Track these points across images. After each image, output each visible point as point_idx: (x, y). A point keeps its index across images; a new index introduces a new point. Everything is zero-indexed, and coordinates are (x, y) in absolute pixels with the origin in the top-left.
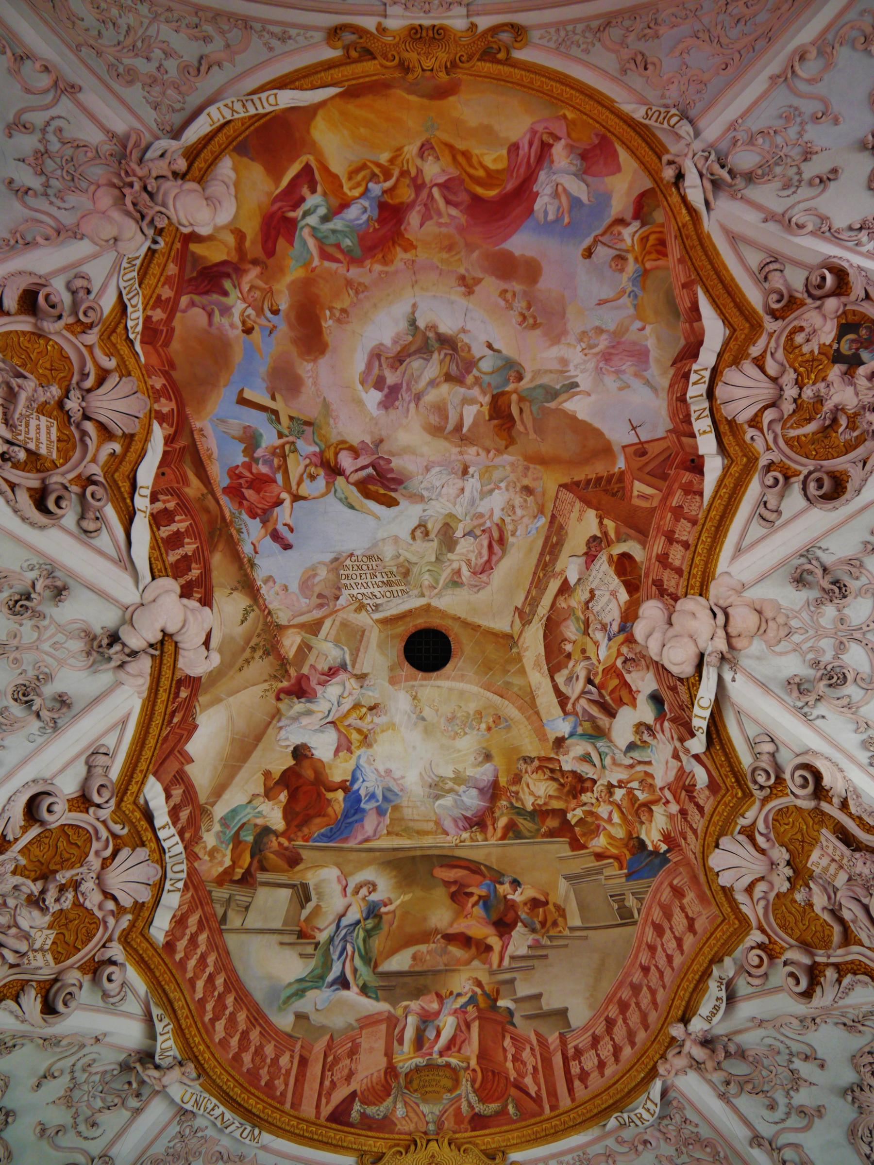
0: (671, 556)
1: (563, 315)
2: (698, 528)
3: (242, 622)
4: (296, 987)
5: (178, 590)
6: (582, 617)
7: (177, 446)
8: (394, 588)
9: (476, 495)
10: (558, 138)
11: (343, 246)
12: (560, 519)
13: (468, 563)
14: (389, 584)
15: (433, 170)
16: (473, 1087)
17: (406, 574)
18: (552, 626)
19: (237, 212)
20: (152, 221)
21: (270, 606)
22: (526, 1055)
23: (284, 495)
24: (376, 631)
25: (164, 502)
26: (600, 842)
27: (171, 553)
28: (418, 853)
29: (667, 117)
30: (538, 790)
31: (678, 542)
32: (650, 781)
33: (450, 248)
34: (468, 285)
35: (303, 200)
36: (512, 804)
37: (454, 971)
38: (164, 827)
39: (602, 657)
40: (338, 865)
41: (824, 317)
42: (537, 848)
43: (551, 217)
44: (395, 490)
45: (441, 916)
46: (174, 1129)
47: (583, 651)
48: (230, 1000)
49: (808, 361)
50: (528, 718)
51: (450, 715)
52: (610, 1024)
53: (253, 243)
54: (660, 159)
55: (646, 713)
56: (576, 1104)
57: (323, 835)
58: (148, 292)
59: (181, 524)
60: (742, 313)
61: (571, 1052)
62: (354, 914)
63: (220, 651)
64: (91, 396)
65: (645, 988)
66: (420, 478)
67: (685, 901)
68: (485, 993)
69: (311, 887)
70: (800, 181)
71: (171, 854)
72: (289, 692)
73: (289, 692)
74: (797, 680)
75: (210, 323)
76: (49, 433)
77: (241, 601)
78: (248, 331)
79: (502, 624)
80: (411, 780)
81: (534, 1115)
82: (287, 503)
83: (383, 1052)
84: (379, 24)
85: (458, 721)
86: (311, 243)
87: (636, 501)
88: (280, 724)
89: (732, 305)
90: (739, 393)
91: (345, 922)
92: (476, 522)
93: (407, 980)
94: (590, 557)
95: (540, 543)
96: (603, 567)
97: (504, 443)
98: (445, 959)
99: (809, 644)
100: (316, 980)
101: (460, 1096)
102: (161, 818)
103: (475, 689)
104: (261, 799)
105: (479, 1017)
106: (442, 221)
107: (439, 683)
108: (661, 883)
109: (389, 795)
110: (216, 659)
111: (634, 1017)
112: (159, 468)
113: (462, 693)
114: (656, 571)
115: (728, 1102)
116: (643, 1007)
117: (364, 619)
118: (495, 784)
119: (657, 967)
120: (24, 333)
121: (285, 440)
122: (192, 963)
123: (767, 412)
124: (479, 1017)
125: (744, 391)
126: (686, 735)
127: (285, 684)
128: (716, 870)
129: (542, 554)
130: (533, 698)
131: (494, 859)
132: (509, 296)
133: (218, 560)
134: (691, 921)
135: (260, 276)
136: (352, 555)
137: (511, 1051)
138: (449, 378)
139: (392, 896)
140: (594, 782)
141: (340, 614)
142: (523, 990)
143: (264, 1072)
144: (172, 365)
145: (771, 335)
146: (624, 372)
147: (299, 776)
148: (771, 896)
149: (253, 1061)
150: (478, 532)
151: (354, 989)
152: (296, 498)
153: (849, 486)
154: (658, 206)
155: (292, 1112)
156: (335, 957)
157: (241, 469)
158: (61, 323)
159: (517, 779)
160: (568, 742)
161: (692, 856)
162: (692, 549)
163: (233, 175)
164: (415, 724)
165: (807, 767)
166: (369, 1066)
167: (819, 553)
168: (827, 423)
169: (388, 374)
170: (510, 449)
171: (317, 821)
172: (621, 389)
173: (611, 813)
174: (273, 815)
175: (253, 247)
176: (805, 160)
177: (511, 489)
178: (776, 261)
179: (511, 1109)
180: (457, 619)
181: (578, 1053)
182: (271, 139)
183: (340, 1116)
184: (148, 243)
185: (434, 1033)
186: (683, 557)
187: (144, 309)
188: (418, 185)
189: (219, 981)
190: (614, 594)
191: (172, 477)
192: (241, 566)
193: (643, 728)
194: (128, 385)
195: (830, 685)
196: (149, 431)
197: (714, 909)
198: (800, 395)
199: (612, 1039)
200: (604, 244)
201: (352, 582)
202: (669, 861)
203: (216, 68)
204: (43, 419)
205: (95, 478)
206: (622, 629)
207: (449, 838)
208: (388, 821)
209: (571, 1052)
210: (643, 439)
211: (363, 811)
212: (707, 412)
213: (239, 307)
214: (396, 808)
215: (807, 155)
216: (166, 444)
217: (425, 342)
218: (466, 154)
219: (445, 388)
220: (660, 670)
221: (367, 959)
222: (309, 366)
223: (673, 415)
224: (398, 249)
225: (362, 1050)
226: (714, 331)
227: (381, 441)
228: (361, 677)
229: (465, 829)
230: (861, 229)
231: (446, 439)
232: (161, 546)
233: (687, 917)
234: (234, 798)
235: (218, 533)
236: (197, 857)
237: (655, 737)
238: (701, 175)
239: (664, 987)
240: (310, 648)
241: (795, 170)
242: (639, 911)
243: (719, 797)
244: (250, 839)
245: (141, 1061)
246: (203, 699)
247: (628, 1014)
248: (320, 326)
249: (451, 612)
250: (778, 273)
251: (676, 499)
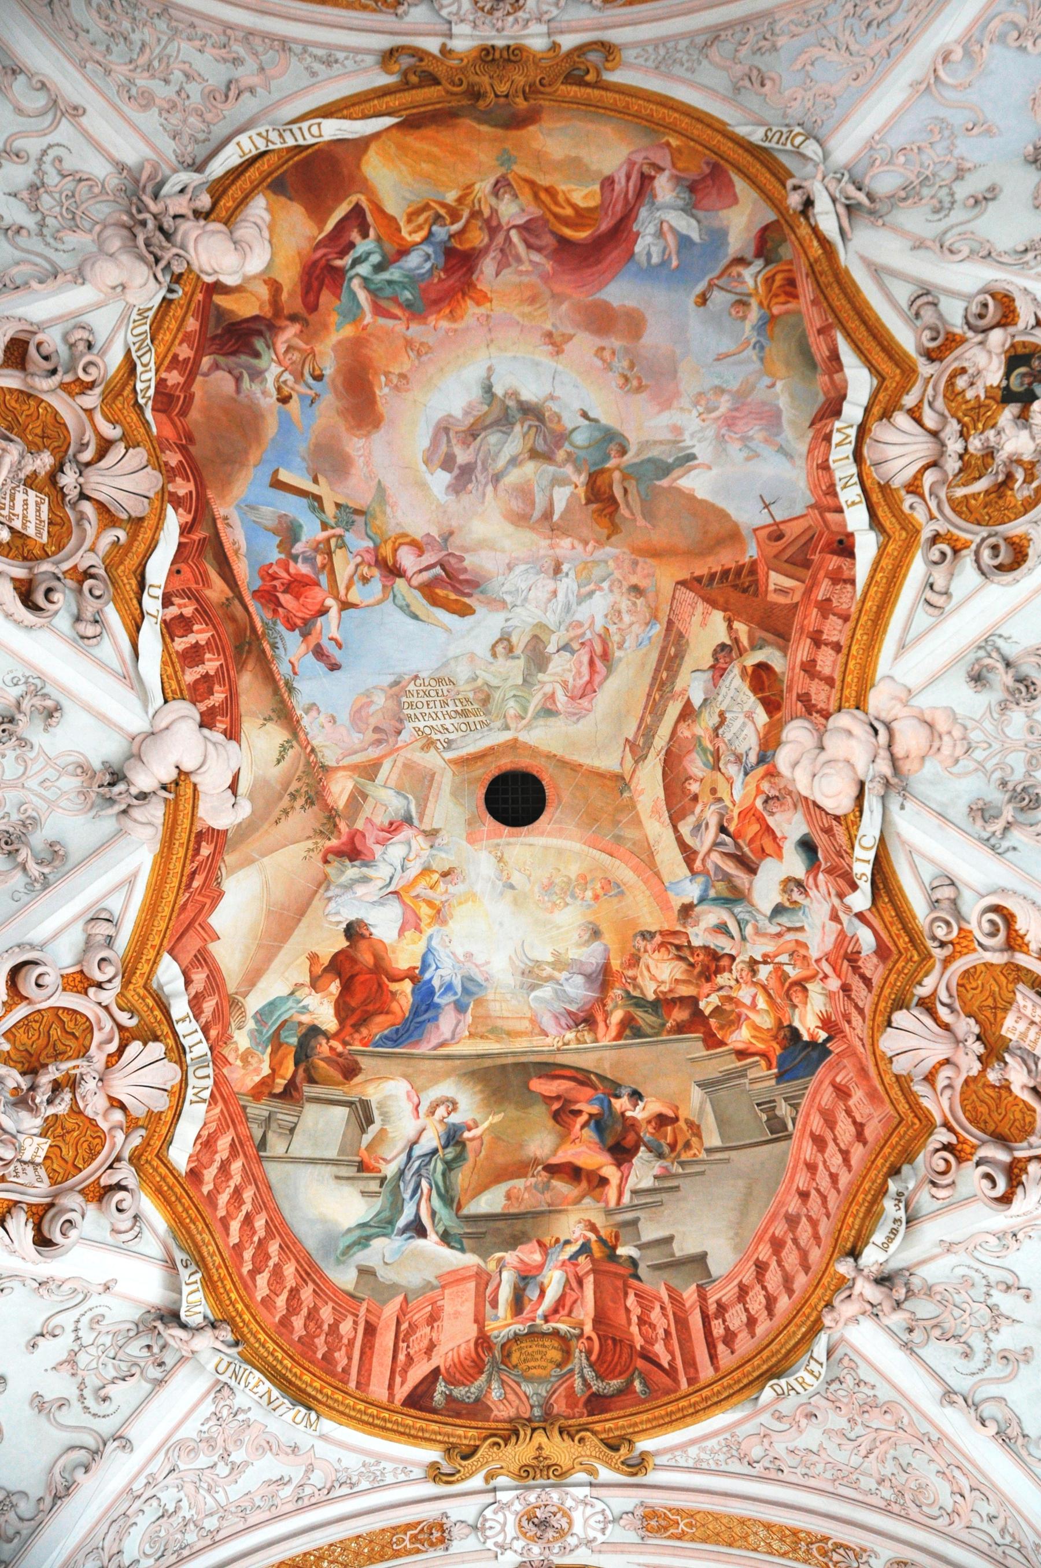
1: (674, 374)
2: (851, 624)
3: (279, 762)
4: (357, 1233)
5: (198, 717)
6: (710, 747)
7: (196, 536)
8: (471, 720)
9: (573, 599)
10: (660, 169)
11: (402, 299)
12: (679, 625)
13: (565, 684)
14: (464, 713)
15: (510, 211)
16: (588, 1359)
17: (486, 701)
18: (671, 761)
19: (272, 260)
20: (168, 265)
21: (315, 743)
22: (655, 1315)
23: (330, 602)
24: (449, 774)
25: (180, 606)
26: (741, 1037)
27: (188, 671)
28: (510, 1060)
29: (791, 137)
30: (661, 974)
32: (803, 952)
33: (533, 300)
34: (555, 343)
35: (352, 245)
36: (628, 992)
37: (560, 1211)
38: (183, 1020)
39: (737, 797)
40: (406, 1077)
41: (989, 352)
42: (661, 1047)
43: (655, 260)
44: (469, 595)
45: (541, 1142)
46: (208, 1408)
47: (714, 791)
48: (273, 1248)
50: (646, 882)
51: (545, 881)
52: (761, 1268)
53: (290, 295)
54: (784, 186)
55: (795, 865)
56: (720, 1374)
57: (386, 1038)
58: (162, 349)
59: (200, 635)
60: (891, 357)
61: (712, 1308)
62: (430, 1141)
63: (251, 797)
65: (804, 1220)
66: (501, 579)
67: (851, 1103)
68: (601, 1240)
69: (374, 1105)
70: (953, 203)
71: (194, 1055)
72: (339, 853)
73: (339, 853)
74: (981, 804)
75: (238, 390)
77: (277, 734)
78: (284, 400)
79: (609, 761)
80: (498, 967)
81: (668, 1392)
82: (334, 612)
83: (472, 1317)
84: (444, 45)
85: (557, 889)
86: (362, 296)
87: (773, 597)
88: (330, 894)
90: (892, 452)
91: (417, 1151)
92: (572, 633)
93: (500, 1224)
94: (718, 671)
95: (655, 655)
96: (735, 685)
97: (605, 532)
98: (548, 1196)
99: (995, 761)
100: (383, 1225)
101: (572, 1370)
102: (180, 1008)
103: (577, 846)
104: (307, 990)
105: (594, 1271)
106: (523, 268)
107: (531, 840)
108: (821, 1082)
109: (470, 986)
110: (245, 809)
111: (791, 1257)
113: (560, 852)
114: (802, 683)
115: (912, 1351)
116: (802, 1244)
117: (432, 760)
118: (606, 968)
119: (818, 1191)
121: (330, 532)
122: (223, 1199)
123: (928, 473)
124: (594, 1271)
126: (846, 888)
127: (334, 842)
128: (890, 1054)
129: (657, 670)
130: (652, 855)
131: (607, 1066)
132: (607, 354)
133: (247, 681)
134: (859, 1127)
135: (300, 335)
136: (416, 677)
137: (636, 1311)
138: (534, 454)
139: (478, 1117)
140: (733, 958)
141: (402, 752)
142: (649, 1232)
143: (320, 1341)
144: (190, 439)
146: (751, 438)
147: (354, 961)
148: (958, 1083)
149: (306, 1326)
150: (575, 646)
151: (433, 1237)
152: (346, 606)
153: (1031, 551)
154: (784, 240)
155: (358, 1394)
156: (407, 1196)
157: (275, 568)
159: (634, 961)
160: (697, 909)
161: (858, 1043)
162: (845, 651)
163: (267, 217)
164: (501, 894)
165: (996, 909)
166: (455, 1336)
167: (1000, 643)
169: (461, 453)
170: (613, 539)
171: (380, 1019)
172: (748, 459)
173: (754, 997)
174: (322, 1010)
175: (291, 299)
176: (957, 179)
177: (616, 590)
178: (928, 293)
179: (637, 1385)
180: (550, 757)
181: (722, 1309)
182: (312, 176)
183: (419, 1400)
184: (163, 293)
185: (537, 1293)
186: (834, 662)
187: (157, 371)
188: (493, 228)
189: (260, 1223)
190: (750, 716)
191: (190, 575)
192: (276, 691)
193: (792, 885)
194: (138, 456)
195: (1022, 809)
196: (161, 518)
197: (889, 1108)
198: (966, 449)
199: (764, 1288)
200: (722, 288)
201: (417, 712)
202: (830, 1052)
203: (247, 95)
206: (762, 760)
207: (549, 1040)
208: (469, 1018)
209: (712, 1308)
210: (778, 519)
211: (437, 1006)
212: (855, 479)
213: (273, 371)
214: (479, 1002)
215: (960, 173)
216: (181, 534)
217: (505, 412)
218: (551, 191)
219: (530, 468)
220: (812, 808)
221: (448, 1199)
222: (361, 442)
223: (814, 487)
224: (469, 302)
225: (445, 1315)
226: (859, 383)
227: (451, 534)
228: (432, 834)
229: (569, 1028)
231: (533, 529)
232: (180, 660)
233: (855, 1122)
234: (272, 987)
235: (247, 647)
236: (226, 1062)
237: (807, 895)
238: (834, 200)
239: (828, 1216)
240: (365, 797)
241: (945, 190)
242: (794, 1120)
243: (890, 964)
244: (294, 1041)
245: (161, 1318)
246: (230, 858)
247: (783, 1254)
248: (374, 394)
249: (544, 748)
251: (822, 591)
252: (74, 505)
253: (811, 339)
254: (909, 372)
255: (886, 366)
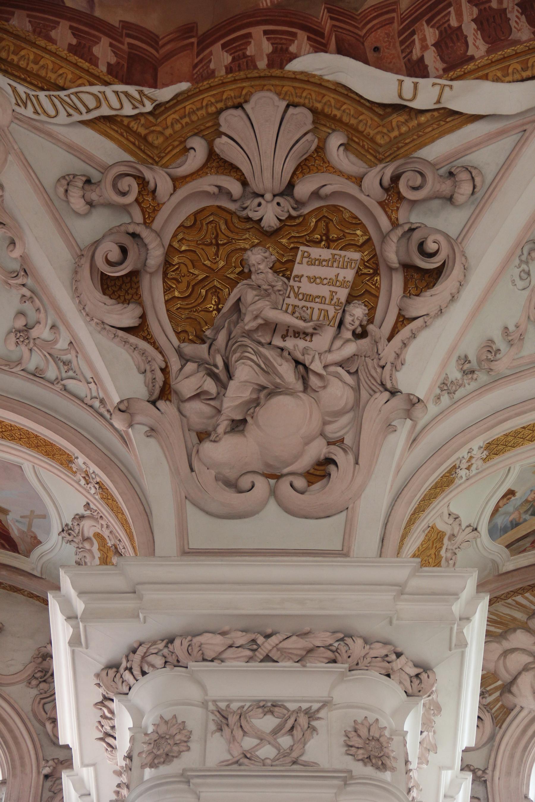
7: (327, 25)
25: (424, 48)
58: (68, 72)
64: (256, 185)
76: (320, 262)
112: (366, 62)
120: (167, 289)
144: (188, 30)
158: (144, 233)
196: (306, 79)
204: (298, 269)
205: (386, 181)
252: (299, 204)
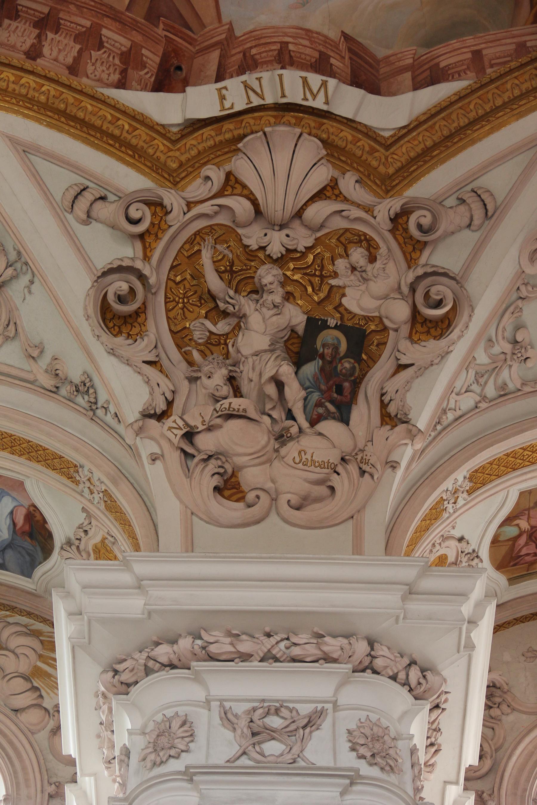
0: (14, 24)
2: (64, 76)
31: (39, 36)
41: (386, 297)
49: (322, 268)
60: (412, 161)
89: (429, 143)
90: (282, 159)
123: (247, 204)
125: (283, 170)
145: (369, 210)
153: (120, 340)
162: (28, 65)
167: (24, 280)
168: (222, 305)
186: (13, 47)
212: (256, 101)
226: (388, 113)
230: (515, 342)
250: (467, 221)
253: (470, 40)
254: (387, 185)
255: (404, 152)
